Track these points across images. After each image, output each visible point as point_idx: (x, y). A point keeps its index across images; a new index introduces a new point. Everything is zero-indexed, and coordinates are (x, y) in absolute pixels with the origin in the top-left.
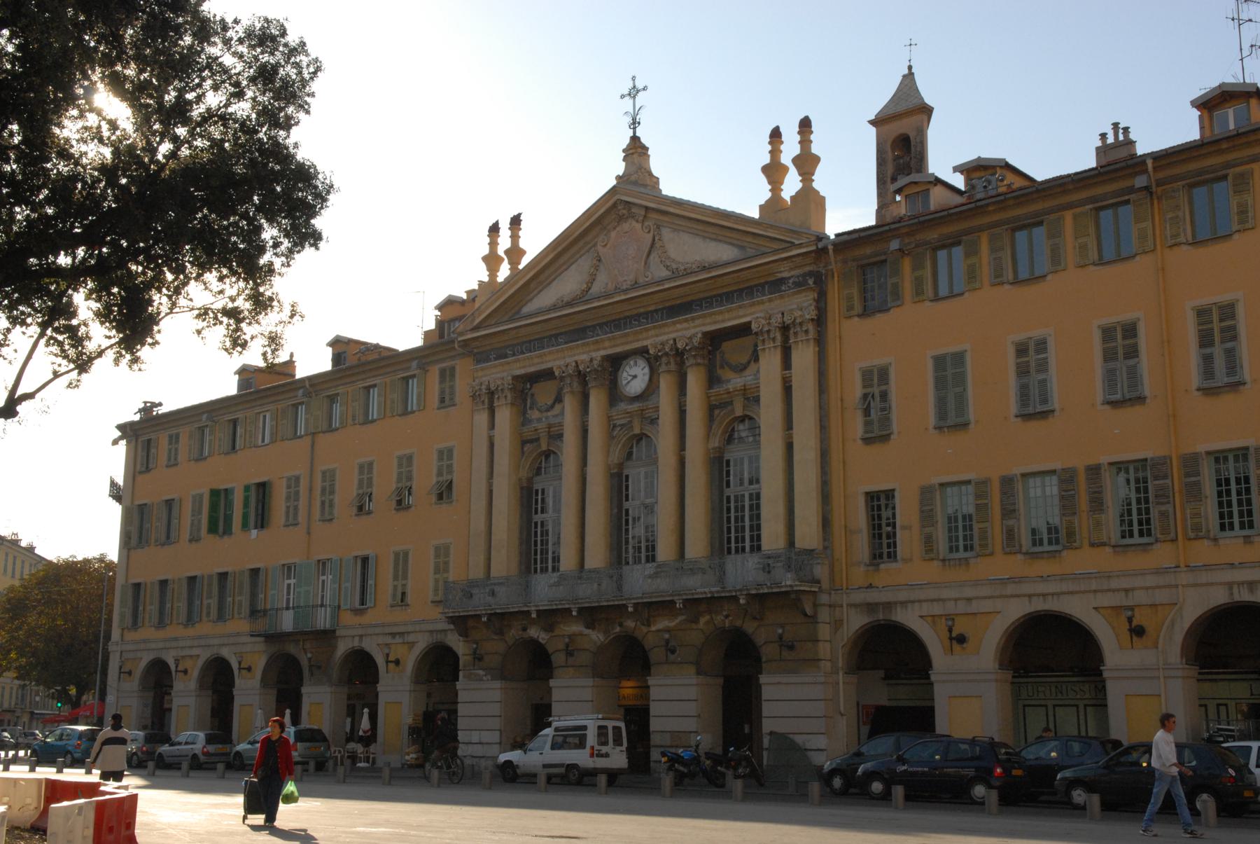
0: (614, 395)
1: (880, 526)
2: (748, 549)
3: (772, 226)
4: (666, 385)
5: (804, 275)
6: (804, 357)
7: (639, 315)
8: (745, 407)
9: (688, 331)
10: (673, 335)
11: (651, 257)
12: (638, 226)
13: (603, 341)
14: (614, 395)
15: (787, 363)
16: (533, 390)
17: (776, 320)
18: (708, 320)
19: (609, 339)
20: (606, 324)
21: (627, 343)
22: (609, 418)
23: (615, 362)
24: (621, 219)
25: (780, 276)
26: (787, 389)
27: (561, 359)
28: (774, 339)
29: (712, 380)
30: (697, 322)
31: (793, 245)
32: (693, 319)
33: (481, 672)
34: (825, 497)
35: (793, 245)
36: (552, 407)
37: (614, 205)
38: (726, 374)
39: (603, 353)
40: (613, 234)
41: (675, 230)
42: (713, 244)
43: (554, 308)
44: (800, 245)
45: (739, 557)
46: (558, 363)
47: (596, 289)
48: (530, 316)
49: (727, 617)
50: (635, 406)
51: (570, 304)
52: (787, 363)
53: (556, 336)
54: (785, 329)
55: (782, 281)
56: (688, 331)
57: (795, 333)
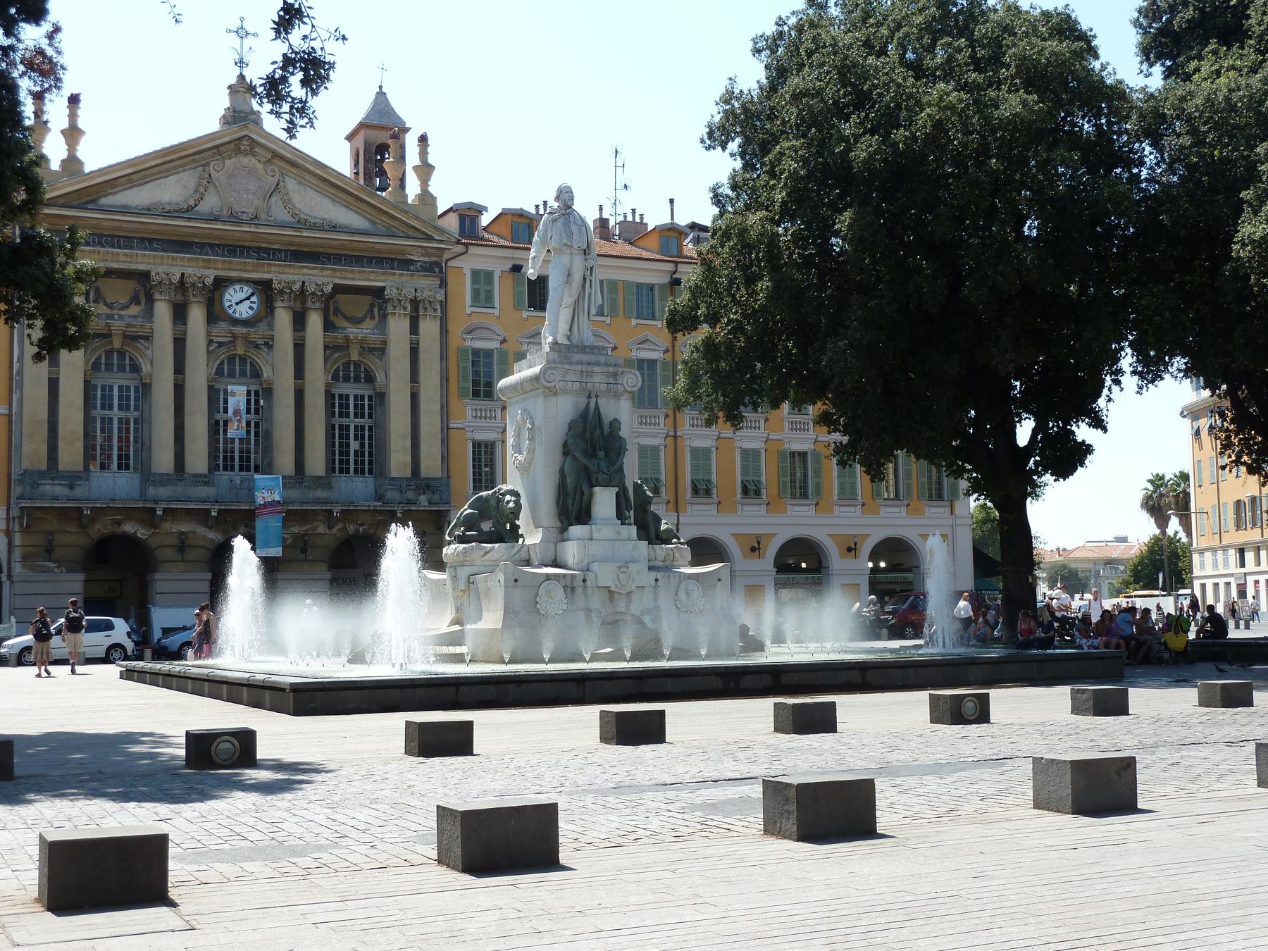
0: (215, 314)
1: (480, 467)
2: (237, 468)
3: (417, 218)
4: (283, 318)
5: (432, 263)
6: (429, 327)
7: (260, 249)
8: (361, 354)
9: (319, 278)
10: (305, 278)
11: (273, 199)
12: (260, 166)
13: (216, 261)
14: (215, 314)
15: (414, 329)
16: (98, 284)
17: (409, 292)
18: (338, 274)
19: (224, 262)
20: (218, 246)
21: (245, 271)
22: (208, 333)
23: (221, 284)
24: (238, 152)
25: (410, 257)
26: (414, 351)
27: (166, 267)
28: (405, 308)
29: (328, 326)
30: (326, 273)
31: (430, 238)
32: (322, 269)
33: (51, 564)
34: (445, 441)
35: (430, 238)
36: (127, 307)
37: (239, 139)
38: (341, 323)
39: (217, 272)
40: (228, 163)
41: (300, 183)
42: (343, 210)
43: (149, 210)
44: (441, 241)
45: (343, 477)
46: (160, 269)
47: (204, 207)
48: (125, 210)
49: (362, 525)
50: (239, 330)
51: (167, 214)
52: (414, 329)
53: (151, 241)
54: (415, 303)
55: (411, 262)
56: (319, 278)
57: (426, 309)
